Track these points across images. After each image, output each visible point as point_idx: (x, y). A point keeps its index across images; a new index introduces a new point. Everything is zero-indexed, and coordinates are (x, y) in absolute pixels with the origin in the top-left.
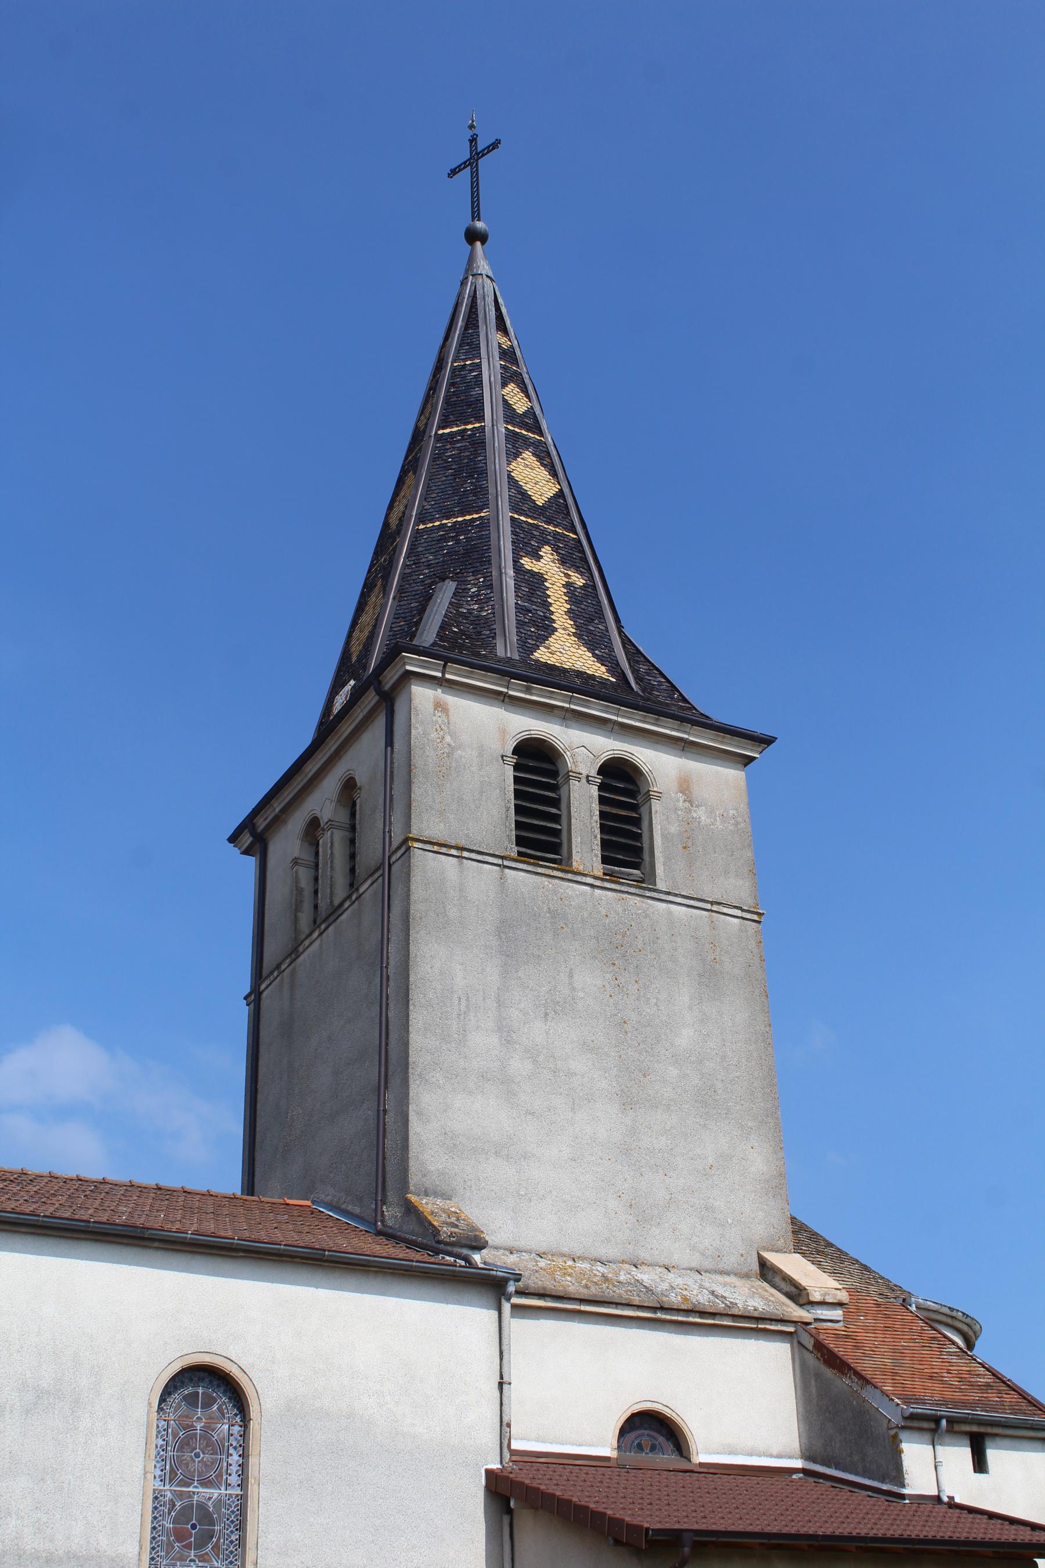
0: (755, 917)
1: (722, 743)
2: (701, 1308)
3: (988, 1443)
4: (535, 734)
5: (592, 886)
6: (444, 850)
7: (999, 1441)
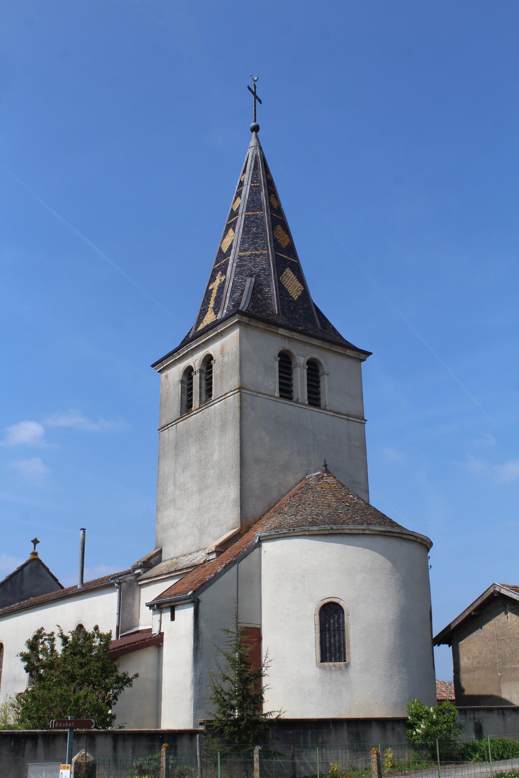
0: (237, 391)
1: (227, 325)
2: (185, 567)
3: (176, 609)
5: (196, 414)
6: (165, 428)
7: (179, 607)
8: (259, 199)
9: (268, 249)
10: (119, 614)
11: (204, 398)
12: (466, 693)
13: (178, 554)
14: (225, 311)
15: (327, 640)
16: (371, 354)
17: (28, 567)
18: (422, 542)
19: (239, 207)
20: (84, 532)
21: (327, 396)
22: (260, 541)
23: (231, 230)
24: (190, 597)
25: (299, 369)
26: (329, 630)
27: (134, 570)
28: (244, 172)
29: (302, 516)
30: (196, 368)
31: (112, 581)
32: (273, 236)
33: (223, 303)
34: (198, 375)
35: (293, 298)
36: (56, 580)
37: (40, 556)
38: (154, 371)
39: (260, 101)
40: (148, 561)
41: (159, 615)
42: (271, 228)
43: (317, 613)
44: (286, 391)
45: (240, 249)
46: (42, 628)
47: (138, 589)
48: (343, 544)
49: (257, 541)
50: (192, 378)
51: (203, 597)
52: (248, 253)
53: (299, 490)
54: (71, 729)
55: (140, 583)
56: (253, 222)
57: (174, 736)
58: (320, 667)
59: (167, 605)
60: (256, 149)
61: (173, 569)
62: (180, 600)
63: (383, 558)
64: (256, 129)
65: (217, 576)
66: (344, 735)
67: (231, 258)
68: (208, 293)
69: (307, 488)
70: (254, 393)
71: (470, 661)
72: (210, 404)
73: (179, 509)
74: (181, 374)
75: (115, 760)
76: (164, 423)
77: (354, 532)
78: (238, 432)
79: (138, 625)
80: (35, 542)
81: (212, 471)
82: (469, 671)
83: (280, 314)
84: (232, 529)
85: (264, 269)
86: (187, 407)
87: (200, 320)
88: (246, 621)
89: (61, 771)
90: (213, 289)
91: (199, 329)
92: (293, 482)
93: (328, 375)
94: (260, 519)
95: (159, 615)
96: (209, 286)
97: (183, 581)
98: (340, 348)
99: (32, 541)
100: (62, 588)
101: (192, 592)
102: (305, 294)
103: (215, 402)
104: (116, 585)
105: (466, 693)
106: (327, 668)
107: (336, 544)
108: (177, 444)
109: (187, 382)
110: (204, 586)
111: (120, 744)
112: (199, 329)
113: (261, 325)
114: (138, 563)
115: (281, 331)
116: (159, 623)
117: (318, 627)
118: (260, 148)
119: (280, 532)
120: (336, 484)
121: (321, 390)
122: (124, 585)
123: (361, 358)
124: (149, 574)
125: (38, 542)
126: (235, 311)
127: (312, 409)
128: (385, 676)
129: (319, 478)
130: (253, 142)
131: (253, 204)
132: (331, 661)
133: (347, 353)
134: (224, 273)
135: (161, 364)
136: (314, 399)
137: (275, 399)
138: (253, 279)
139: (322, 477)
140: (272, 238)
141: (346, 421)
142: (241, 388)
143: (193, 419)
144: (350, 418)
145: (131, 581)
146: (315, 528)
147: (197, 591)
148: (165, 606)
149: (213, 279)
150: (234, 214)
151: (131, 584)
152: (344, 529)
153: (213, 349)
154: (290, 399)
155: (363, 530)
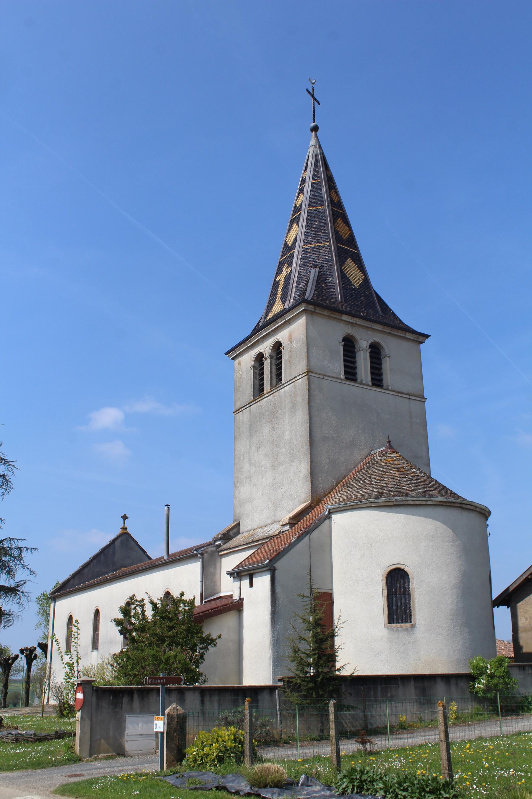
0: (305, 374)
2: (261, 538)
3: (254, 576)
4: (258, 353)
5: (268, 396)
7: (257, 575)
8: (321, 195)
9: (330, 242)
10: (202, 582)
11: (274, 382)
12: (525, 650)
13: (255, 526)
14: (292, 301)
15: (394, 603)
16: (429, 336)
17: (119, 540)
18: (481, 511)
19: (302, 203)
20: (168, 508)
21: (388, 378)
22: (330, 513)
23: (295, 224)
24: (266, 566)
25: (362, 352)
26: (396, 594)
27: (215, 541)
28: (306, 169)
29: (368, 489)
30: (267, 354)
31: (195, 552)
32: (335, 229)
33: (289, 293)
34: (268, 361)
35: (355, 286)
36: (144, 552)
37: (129, 531)
38: (228, 358)
39: (318, 102)
40: (227, 533)
41: (239, 582)
42: (332, 221)
43: (385, 578)
44: (351, 373)
45: (304, 242)
46: (134, 595)
47: (219, 559)
48: (407, 514)
49: (327, 513)
50: (263, 364)
51: (278, 565)
52: (312, 246)
53: (365, 465)
54: (163, 685)
55: (220, 554)
56: (315, 216)
57: (255, 692)
58: (388, 628)
59: (246, 573)
60: (316, 147)
61: (250, 540)
62: (258, 569)
63: (445, 527)
64: (315, 129)
65: (291, 546)
66: (411, 689)
67: (296, 251)
68: (276, 284)
69: (372, 463)
70: (321, 376)
71: (528, 621)
72: (281, 387)
73: (255, 485)
74: (253, 360)
75: (203, 713)
76: (238, 406)
77: (417, 503)
78: (307, 412)
79: (220, 592)
80: (125, 517)
81: (284, 450)
82: (526, 630)
83: (343, 301)
84: (304, 503)
85: (327, 260)
86: (259, 390)
87: (269, 310)
88: (320, 587)
89: (155, 722)
90: (280, 280)
91: (268, 318)
92: (360, 458)
93: (389, 357)
94: (330, 492)
95: (239, 582)
96: (276, 277)
97: (259, 551)
98: (399, 331)
99: (122, 517)
100: (150, 559)
101: (268, 561)
102: (366, 282)
103: (284, 385)
104: (199, 555)
105: (525, 650)
106: (395, 629)
107: (401, 515)
108: (251, 425)
109: (258, 368)
110: (279, 555)
111: (207, 698)
112: (268, 318)
113: (326, 313)
114: (218, 535)
115: (345, 317)
116: (239, 590)
117: (385, 591)
118: (320, 146)
119: (348, 505)
120: (400, 459)
121: (384, 371)
122: (206, 555)
123: (420, 340)
124: (228, 545)
125: (127, 518)
126: (301, 300)
127: (376, 389)
128: (449, 635)
129: (383, 453)
130: (313, 142)
131: (315, 199)
132: (398, 622)
133: (407, 336)
134: (290, 265)
135: (234, 352)
136: (377, 380)
137: (340, 381)
138: (317, 270)
139: (386, 453)
140: (333, 231)
141: (407, 400)
142: (308, 372)
143: (265, 402)
144: (411, 397)
145: (212, 551)
146: (380, 500)
147: (273, 561)
148: (244, 574)
149: (279, 271)
150: (297, 209)
151: (212, 554)
152: (408, 501)
153: (282, 336)
154: (355, 380)
155: (425, 501)
